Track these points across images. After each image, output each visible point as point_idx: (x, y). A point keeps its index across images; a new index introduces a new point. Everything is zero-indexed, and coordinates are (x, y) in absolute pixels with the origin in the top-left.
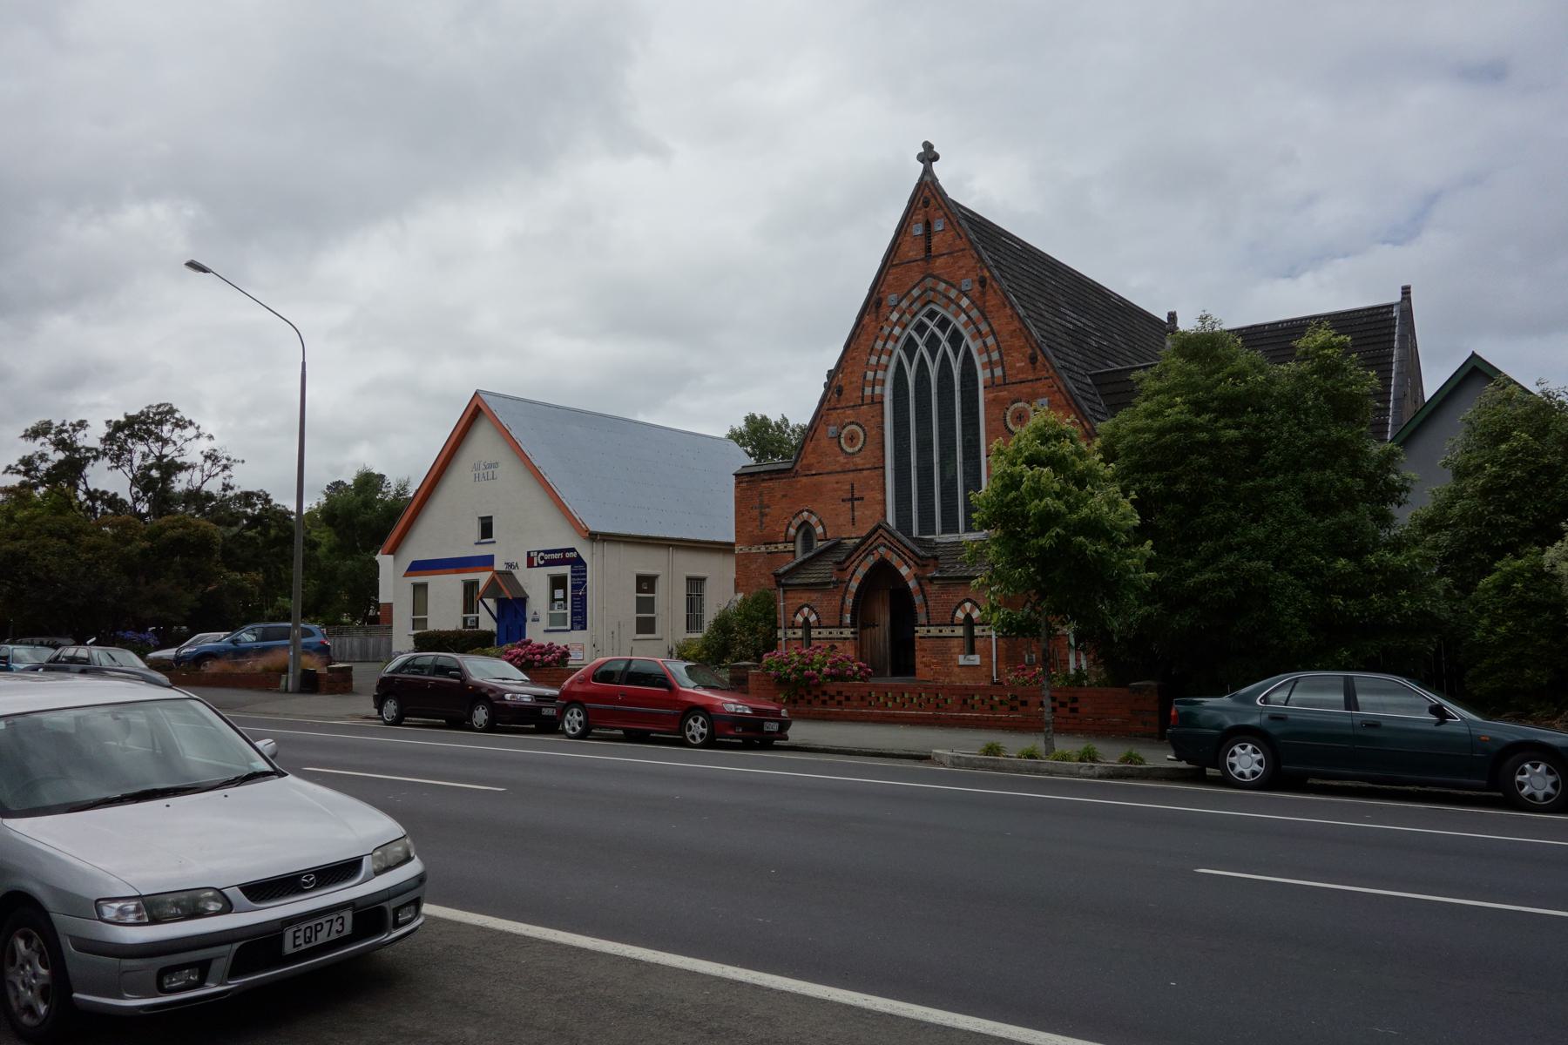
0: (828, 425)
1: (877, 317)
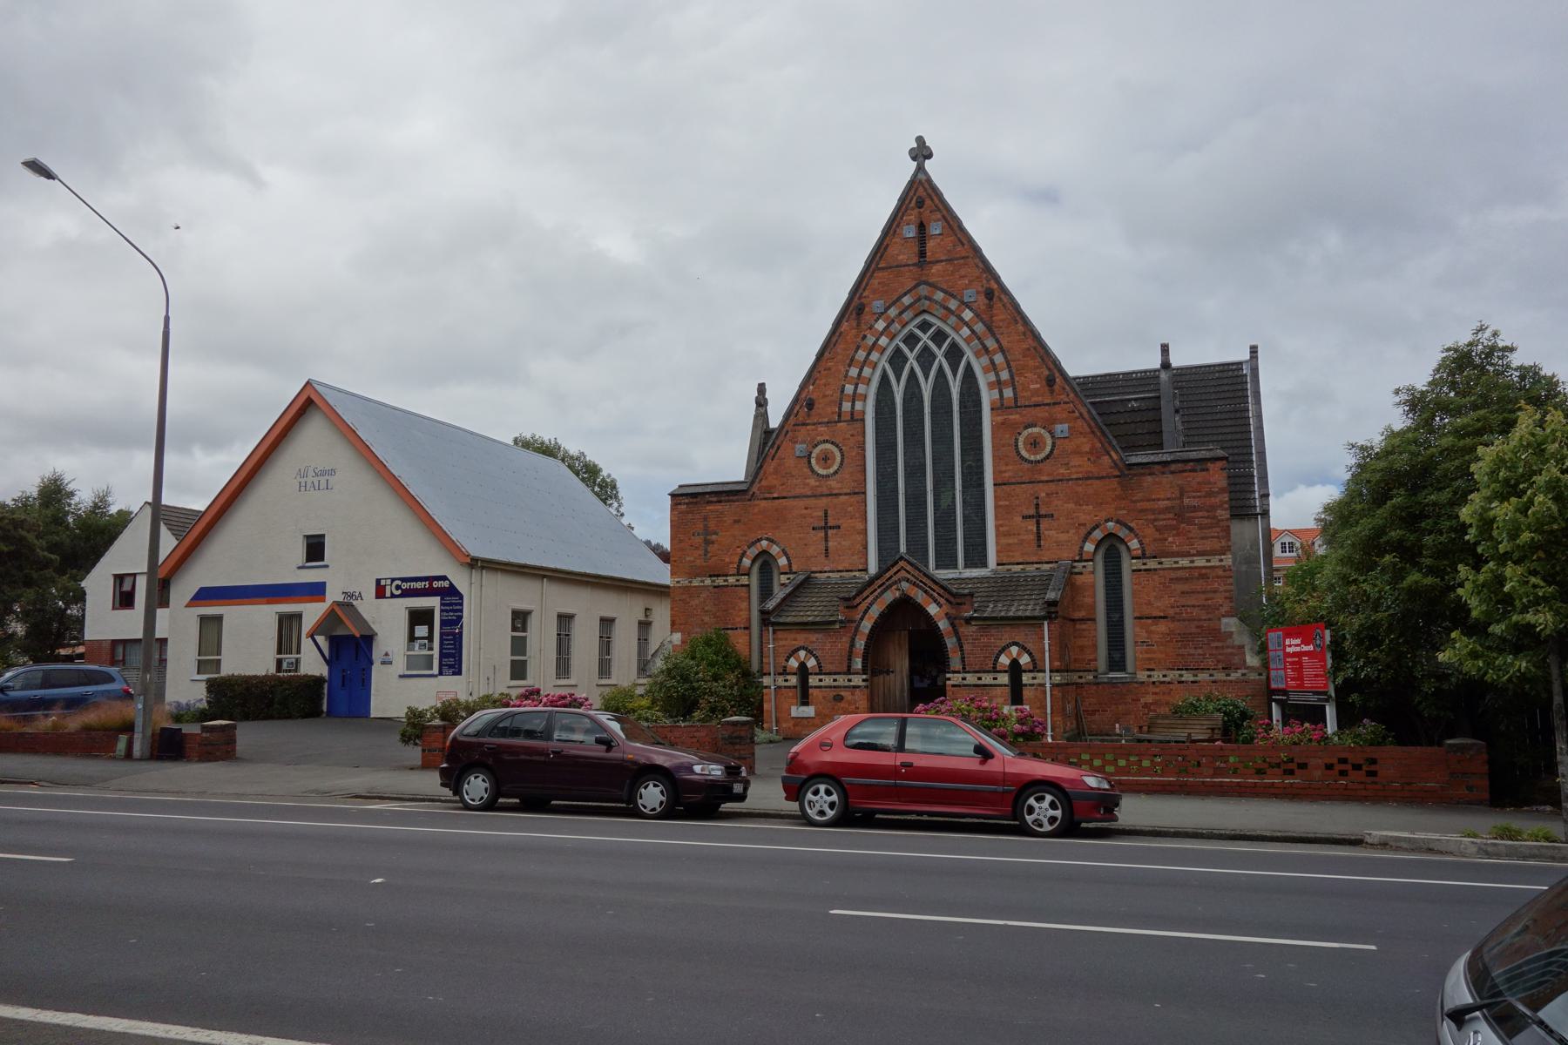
0: (796, 442)
1: (858, 325)
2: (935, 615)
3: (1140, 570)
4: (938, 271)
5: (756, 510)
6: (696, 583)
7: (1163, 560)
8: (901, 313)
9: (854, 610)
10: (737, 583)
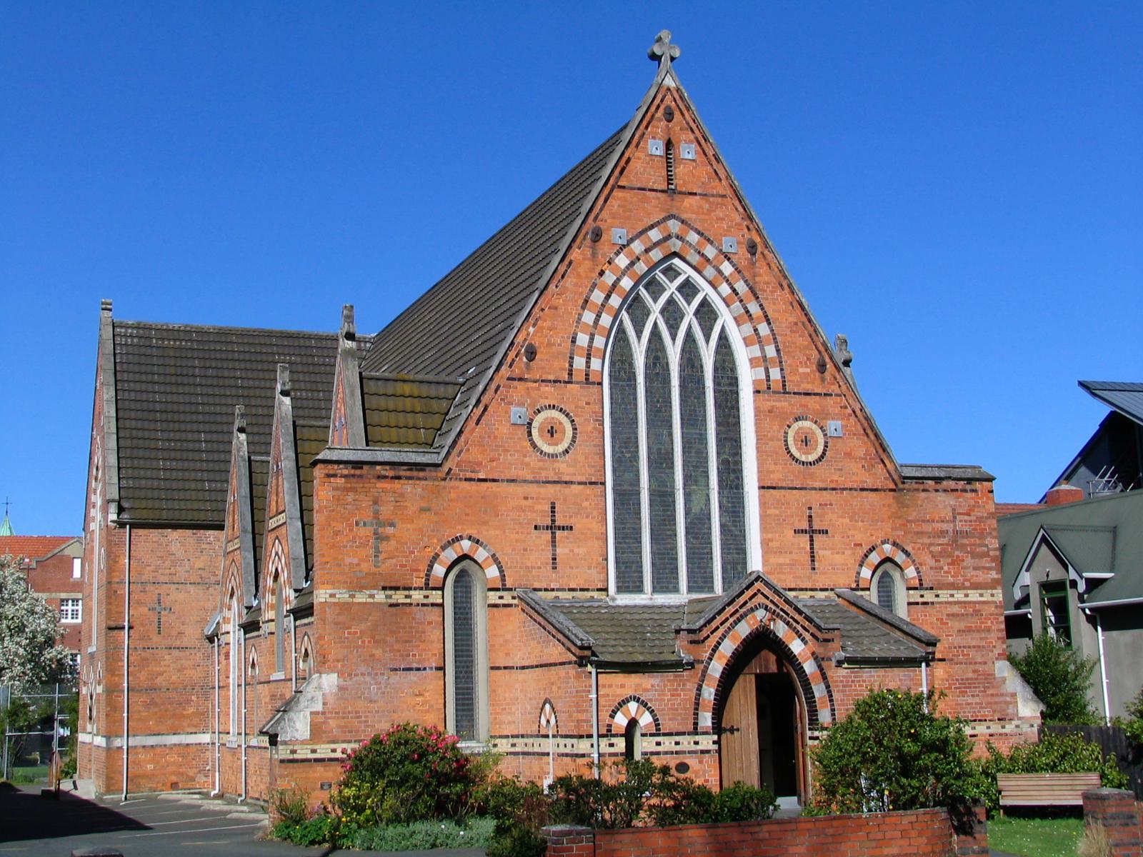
0: (510, 403)
1: (594, 255)
2: (800, 654)
3: (917, 603)
4: (691, 205)
5: (453, 496)
6: (361, 598)
7: (939, 592)
8: (647, 251)
9: (701, 645)
10: (425, 601)
